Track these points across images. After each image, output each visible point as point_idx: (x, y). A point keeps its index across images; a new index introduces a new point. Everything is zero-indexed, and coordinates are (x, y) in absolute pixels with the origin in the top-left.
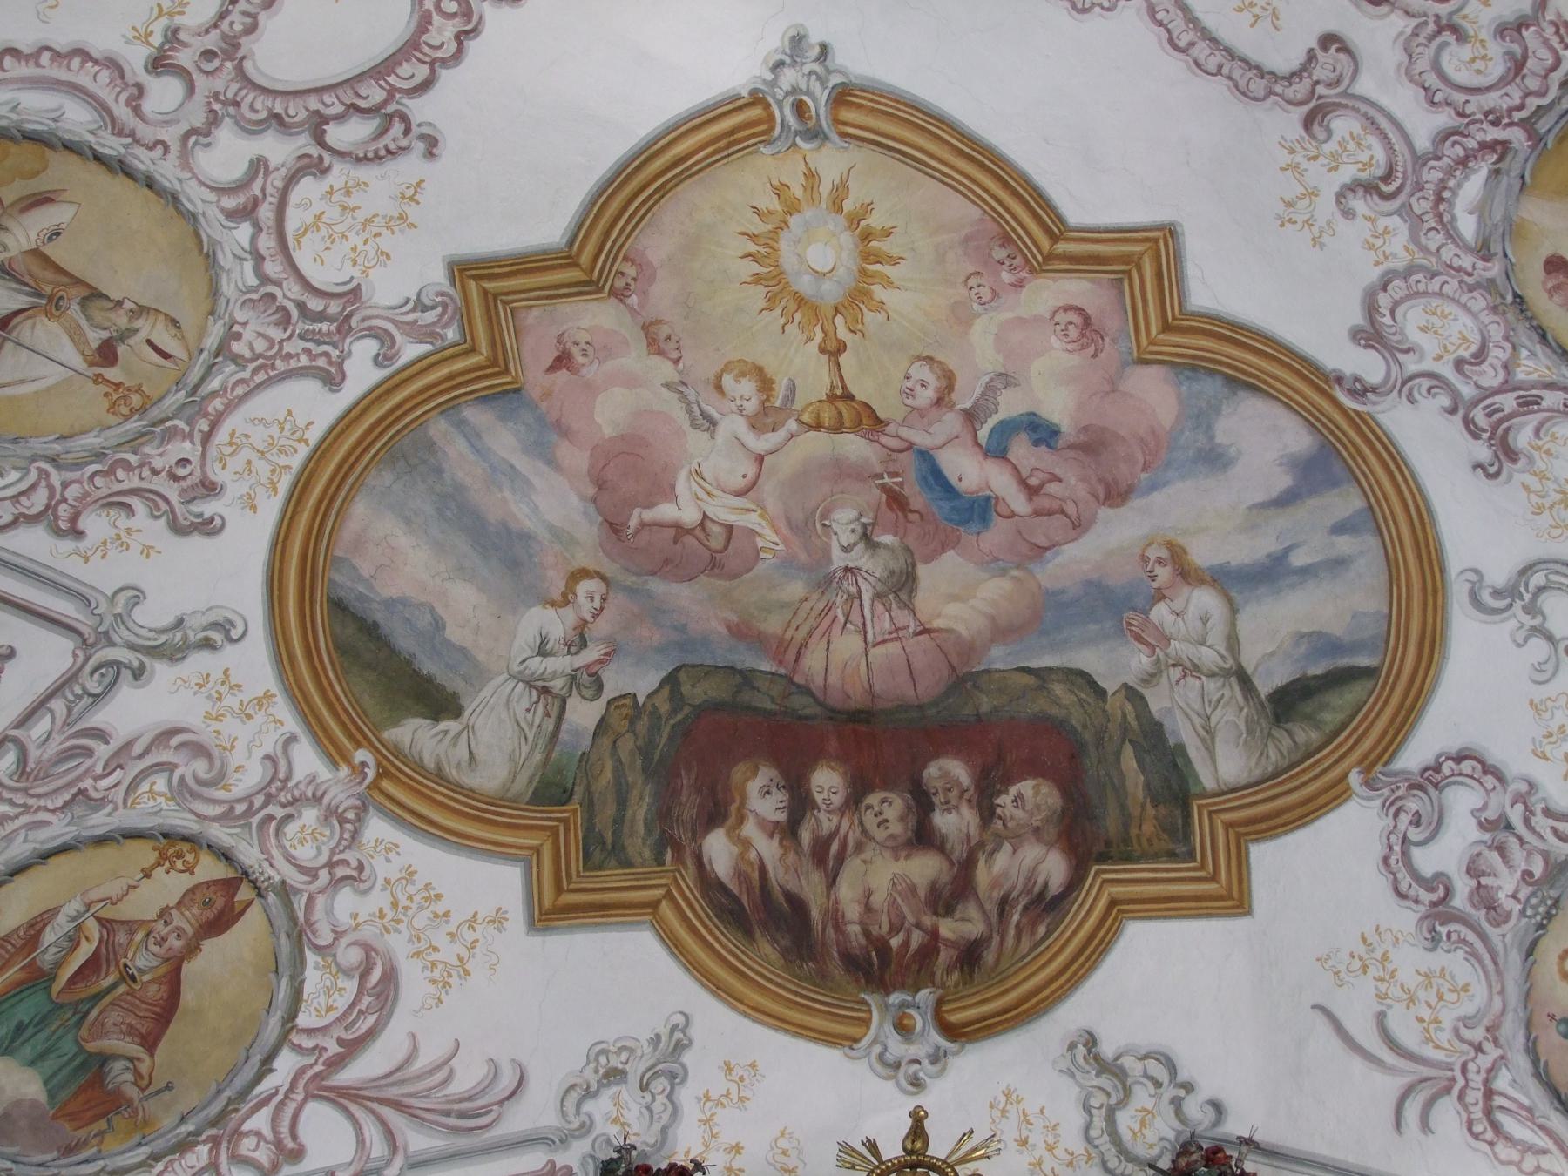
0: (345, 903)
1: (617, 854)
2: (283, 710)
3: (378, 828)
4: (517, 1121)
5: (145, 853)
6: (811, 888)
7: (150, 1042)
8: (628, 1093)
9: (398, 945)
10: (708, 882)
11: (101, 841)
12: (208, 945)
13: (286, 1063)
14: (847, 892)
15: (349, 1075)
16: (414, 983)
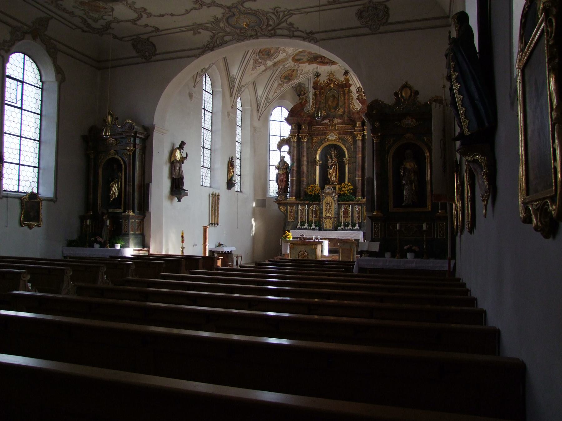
0: (299, 68)
1: (312, 62)
2: (294, 63)
3: (300, 65)
4: (310, 71)
5: (289, 71)
6: (323, 61)
7: (292, 77)
8: (316, 69)
9: (302, 68)
10: (318, 62)
11: (287, 71)
12: (293, 73)
13: (298, 75)
14: (325, 61)
15: (302, 73)
16: (303, 69)
